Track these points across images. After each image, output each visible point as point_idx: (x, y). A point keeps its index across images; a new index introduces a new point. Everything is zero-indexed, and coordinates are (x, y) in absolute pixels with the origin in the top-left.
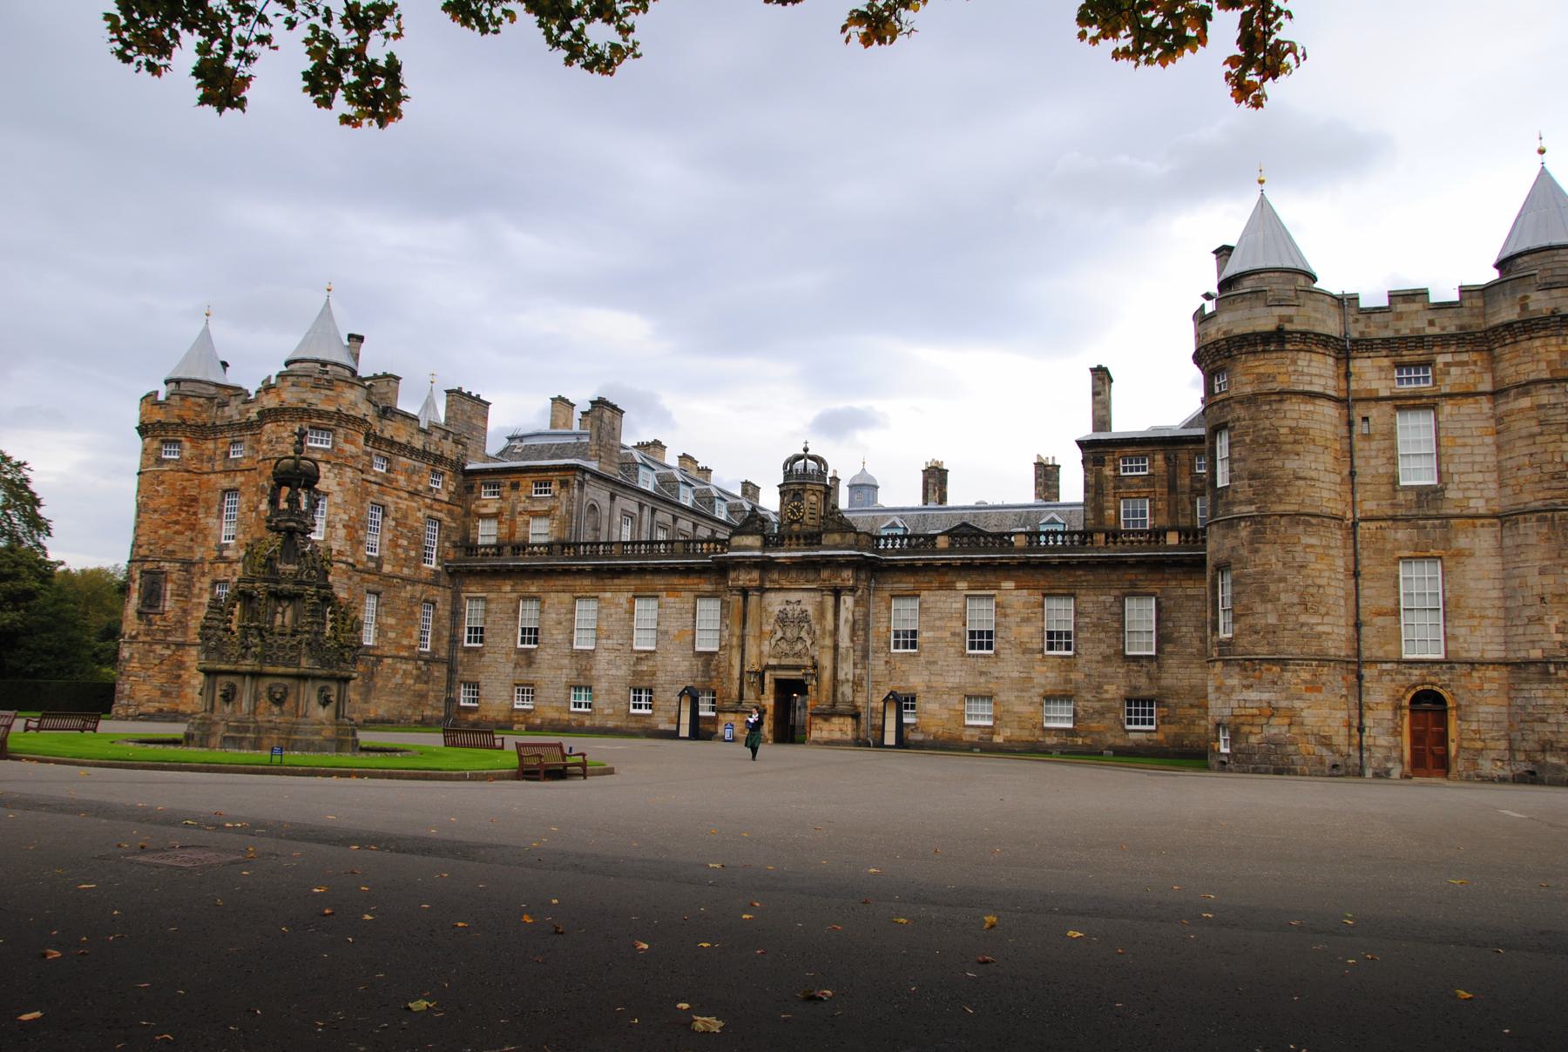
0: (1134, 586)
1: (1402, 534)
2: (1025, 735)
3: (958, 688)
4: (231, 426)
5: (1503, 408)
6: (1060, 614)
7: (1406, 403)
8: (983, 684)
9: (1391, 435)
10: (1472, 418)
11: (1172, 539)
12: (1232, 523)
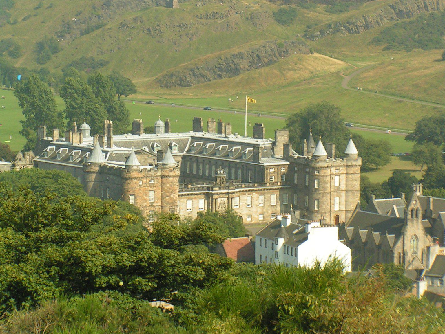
0: (273, 193)
1: (335, 193)
2: (256, 222)
3: (246, 214)
4: (152, 176)
5: (347, 176)
6: (262, 198)
7: (336, 175)
8: (250, 213)
9: (335, 179)
10: (343, 177)
11: (279, 184)
12: (319, 194)
